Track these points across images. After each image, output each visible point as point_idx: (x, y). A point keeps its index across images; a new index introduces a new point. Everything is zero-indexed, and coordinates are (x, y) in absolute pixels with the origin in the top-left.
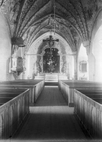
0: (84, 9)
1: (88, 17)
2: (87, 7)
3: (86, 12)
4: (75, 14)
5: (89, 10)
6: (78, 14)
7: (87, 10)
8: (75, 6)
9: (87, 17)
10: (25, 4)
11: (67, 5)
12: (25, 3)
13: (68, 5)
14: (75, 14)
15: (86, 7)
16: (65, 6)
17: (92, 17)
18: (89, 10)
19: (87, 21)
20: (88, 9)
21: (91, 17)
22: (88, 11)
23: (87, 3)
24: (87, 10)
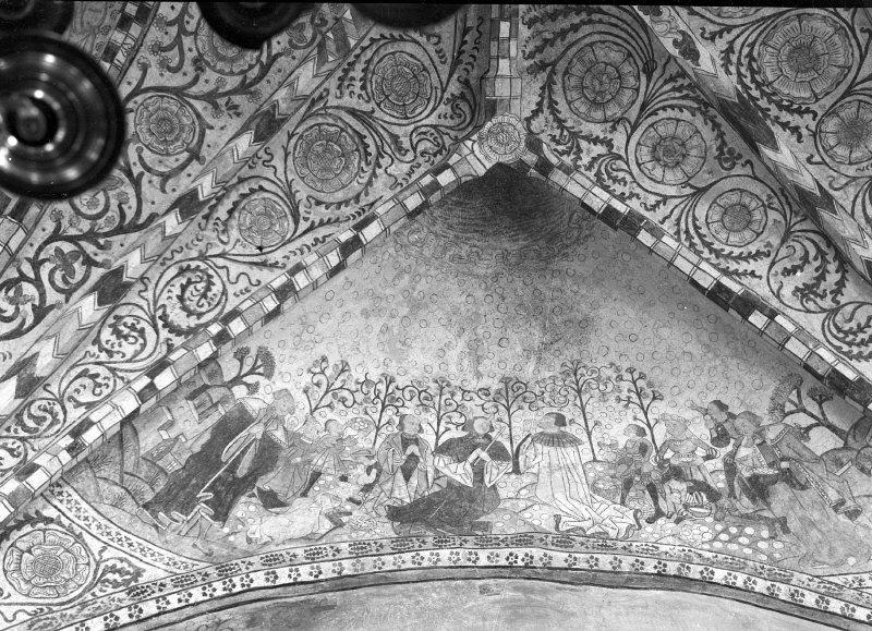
0: (241, 355)
1: (173, 464)
2: (279, 385)
3: (216, 394)
4: (71, 239)
5: (256, 431)
6: (112, 289)
7: (240, 391)
8: (222, 213)
9: (149, 439)
11: (176, 81)
13: (179, 92)
14: (71, 239)
15: (266, 363)
16: (144, 54)
17: (221, 511)
18: (256, 431)
19: (85, 480)
20: (254, 405)
21: (203, 511)
22: (242, 420)
23: (320, 350)
24: (242, 410)
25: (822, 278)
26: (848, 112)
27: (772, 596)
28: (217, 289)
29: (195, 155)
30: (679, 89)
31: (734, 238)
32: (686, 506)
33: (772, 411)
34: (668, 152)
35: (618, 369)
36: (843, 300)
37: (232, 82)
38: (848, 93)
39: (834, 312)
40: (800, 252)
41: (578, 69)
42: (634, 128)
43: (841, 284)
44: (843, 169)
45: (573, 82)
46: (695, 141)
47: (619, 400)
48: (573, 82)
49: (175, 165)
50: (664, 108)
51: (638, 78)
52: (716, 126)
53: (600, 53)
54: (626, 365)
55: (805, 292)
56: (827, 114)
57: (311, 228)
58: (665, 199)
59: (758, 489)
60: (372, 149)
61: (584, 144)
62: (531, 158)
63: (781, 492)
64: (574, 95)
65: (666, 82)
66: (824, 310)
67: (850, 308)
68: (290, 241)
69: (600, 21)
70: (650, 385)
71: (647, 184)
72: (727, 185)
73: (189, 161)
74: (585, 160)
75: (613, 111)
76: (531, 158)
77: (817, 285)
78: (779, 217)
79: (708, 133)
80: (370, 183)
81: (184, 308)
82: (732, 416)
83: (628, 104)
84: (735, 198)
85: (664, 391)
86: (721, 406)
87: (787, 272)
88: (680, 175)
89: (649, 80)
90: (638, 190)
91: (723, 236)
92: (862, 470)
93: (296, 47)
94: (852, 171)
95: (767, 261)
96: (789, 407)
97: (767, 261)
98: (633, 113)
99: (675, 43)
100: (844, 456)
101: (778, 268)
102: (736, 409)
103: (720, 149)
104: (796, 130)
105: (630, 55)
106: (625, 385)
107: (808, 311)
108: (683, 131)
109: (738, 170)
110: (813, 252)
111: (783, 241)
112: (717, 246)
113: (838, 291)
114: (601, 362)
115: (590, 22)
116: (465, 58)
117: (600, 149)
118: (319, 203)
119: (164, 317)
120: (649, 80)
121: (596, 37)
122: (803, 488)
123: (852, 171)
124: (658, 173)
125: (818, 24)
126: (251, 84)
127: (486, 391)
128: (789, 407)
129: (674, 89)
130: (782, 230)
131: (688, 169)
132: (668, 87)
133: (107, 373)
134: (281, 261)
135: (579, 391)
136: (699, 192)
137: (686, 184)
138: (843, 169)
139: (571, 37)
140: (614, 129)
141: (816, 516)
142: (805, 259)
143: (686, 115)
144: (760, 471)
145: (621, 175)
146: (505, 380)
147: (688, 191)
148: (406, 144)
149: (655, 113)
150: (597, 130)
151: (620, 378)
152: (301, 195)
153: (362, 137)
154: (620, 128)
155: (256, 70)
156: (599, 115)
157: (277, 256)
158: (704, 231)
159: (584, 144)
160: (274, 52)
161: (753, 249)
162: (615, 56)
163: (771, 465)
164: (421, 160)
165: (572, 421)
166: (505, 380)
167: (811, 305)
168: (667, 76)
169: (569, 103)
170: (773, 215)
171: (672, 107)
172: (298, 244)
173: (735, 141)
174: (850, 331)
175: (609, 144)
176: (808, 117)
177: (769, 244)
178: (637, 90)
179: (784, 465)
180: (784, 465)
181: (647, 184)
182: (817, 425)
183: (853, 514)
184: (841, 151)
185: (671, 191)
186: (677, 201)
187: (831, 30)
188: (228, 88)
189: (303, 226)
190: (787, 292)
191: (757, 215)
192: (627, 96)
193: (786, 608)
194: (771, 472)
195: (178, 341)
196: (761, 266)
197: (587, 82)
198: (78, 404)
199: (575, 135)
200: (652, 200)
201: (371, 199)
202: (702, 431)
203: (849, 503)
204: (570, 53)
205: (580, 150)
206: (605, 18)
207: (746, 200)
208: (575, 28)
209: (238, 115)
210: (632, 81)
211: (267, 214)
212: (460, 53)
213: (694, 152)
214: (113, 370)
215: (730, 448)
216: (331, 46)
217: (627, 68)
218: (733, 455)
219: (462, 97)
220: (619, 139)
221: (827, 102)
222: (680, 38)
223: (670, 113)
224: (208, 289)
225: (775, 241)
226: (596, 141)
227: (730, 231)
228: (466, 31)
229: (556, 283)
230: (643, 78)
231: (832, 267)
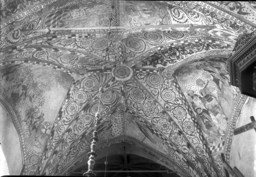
10: (190, 53)
12: (189, 55)
25: (67, 122)
26: (90, 117)
27: (22, 143)
28: (42, 56)
29: (65, 46)
30: (90, 96)
31: (69, 109)
32: (28, 123)
33: (45, 122)
34: (80, 96)
35: (44, 98)
36: (64, 126)
37: (79, 45)
38: (93, 116)
39: (62, 125)
40: (69, 118)
41: (91, 80)
42: (83, 91)
43: (66, 125)
44: (82, 119)
45: (89, 79)
46: (83, 99)
47: (39, 101)
48: (89, 79)
49: (62, 44)
50: (87, 94)
51: (91, 90)
52: (85, 102)
53: (94, 83)
54: (45, 98)
55: (64, 121)
56: (90, 114)
57: (56, 60)
58: (73, 99)
59: (34, 127)
60: (72, 61)
61: (79, 85)
62: (75, 81)
63: (35, 130)
64: (87, 80)
65: (91, 94)
66: (62, 124)
67: (63, 127)
68: (53, 59)
69: (98, 83)
70: (43, 103)
71: (75, 95)
72: (77, 105)
73: (63, 45)
74: (77, 86)
75: (85, 87)
76: (75, 81)
77: (65, 122)
78: (74, 114)
79: (84, 101)
80: (66, 63)
81: (37, 54)
82: (43, 117)
83: (87, 88)
84: (75, 107)
85: (43, 106)
86: (44, 115)
87: (66, 118)
88: (77, 99)
89: (91, 91)
90: (74, 95)
91: (69, 108)
92: (42, 137)
93: (87, 50)
94: (82, 120)
95: (67, 114)
96: (47, 124)
97: (67, 114)
98: (85, 90)
99: (97, 96)
100: (43, 134)
101: (66, 116)
102: (44, 117)
103: (82, 103)
104: (87, 112)
105: (94, 87)
106: (42, 100)
107: (61, 122)
108: (84, 98)
109: (80, 106)
110: (70, 120)
111: (71, 115)
112: (68, 108)
113: (65, 125)
114: (44, 95)
115: (98, 81)
116: (90, 66)
117: (79, 87)
118: (60, 59)
119: (34, 53)
120: (91, 91)
121: (96, 82)
122: (36, 132)
123: (82, 120)
124: (77, 96)
125: (102, 109)
126: (79, 47)
127: (34, 81)
128: (47, 124)
129: (90, 95)
130: (72, 115)
131: (78, 99)
132: (90, 94)
133: (22, 55)
134: (49, 59)
135: (39, 95)
136: (75, 102)
137: (76, 100)
138: (82, 119)
139: (95, 78)
140: (82, 88)
141: (33, 137)
142: (69, 119)
143: (86, 98)
144: (36, 126)
145: (76, 92)
146: (36, 83)
147: (75, 100)
148: (74, 64)
149: (86, 93)
150: (82, 86)
151: (43, 99)
152: (61, 56)
153: (74, 60)
154: (83, 89)
155: (82, 47)
156: (84, 85)
157: (50, 58)
158: (70, 105)
159: (79, 85)
160: (86, 48)
161: (69, 112)
162: (94, 85)
163: (38, 126)
164: (72, 67)
165: (34, 98)
166: (36, 83)
167: (62, 122)
168: (92, 94)
169: (85, 80)
170: (74, 113)
171: (87, 96)
172: (53, 59)
173: (84, 105)
174: (60, 128)
175: (80, 88)
176: (89, 112)
177: (70, 114)
178: (89, 90)
179: (38, 128)
180: (38, 128)
181: (75, 95)
182: (45, 129)
183: (35, 140)
184: (85, 118)
185: (75, 99)
186: (73, 100)
187: (101, 111)
188: (78, 45)
189: (56, 59)
190: (63, 119)
191: (74, 111)
192: (88, 88)
193: (21, 145)
194: (37, 127)
195: (31, 57)
196: (66, 114)
197: (89, 82)
198: (16, 56)
199: (80, 83)
200: (73, 97)
201: (63, 64)
202: (39, 115)
203: (36, 139)
204: (93, 78)
205: (78, 85)
206: (99, 83)
207: (75, 109)
208: (97, 79)
209: (73, 47)
210: (90, 89)
211: (57, 54)
212: (91, 65)
213: (81, 100)
214: (23, 55)
215: (38, 120)
216: (88, 57)
217: (92, 87)
218: (37, 121)
219: (83, 67)
220: (81, 89)
221: (91, 114)
222: (97, 97)
223: (86, 95)
224: (41, 55)
225: (70, 114)
226: (80, 86)
227: (70, 108)
228: (94, 66)
229: (55, 83)
230: (91, 90)
231: (68, 123)
